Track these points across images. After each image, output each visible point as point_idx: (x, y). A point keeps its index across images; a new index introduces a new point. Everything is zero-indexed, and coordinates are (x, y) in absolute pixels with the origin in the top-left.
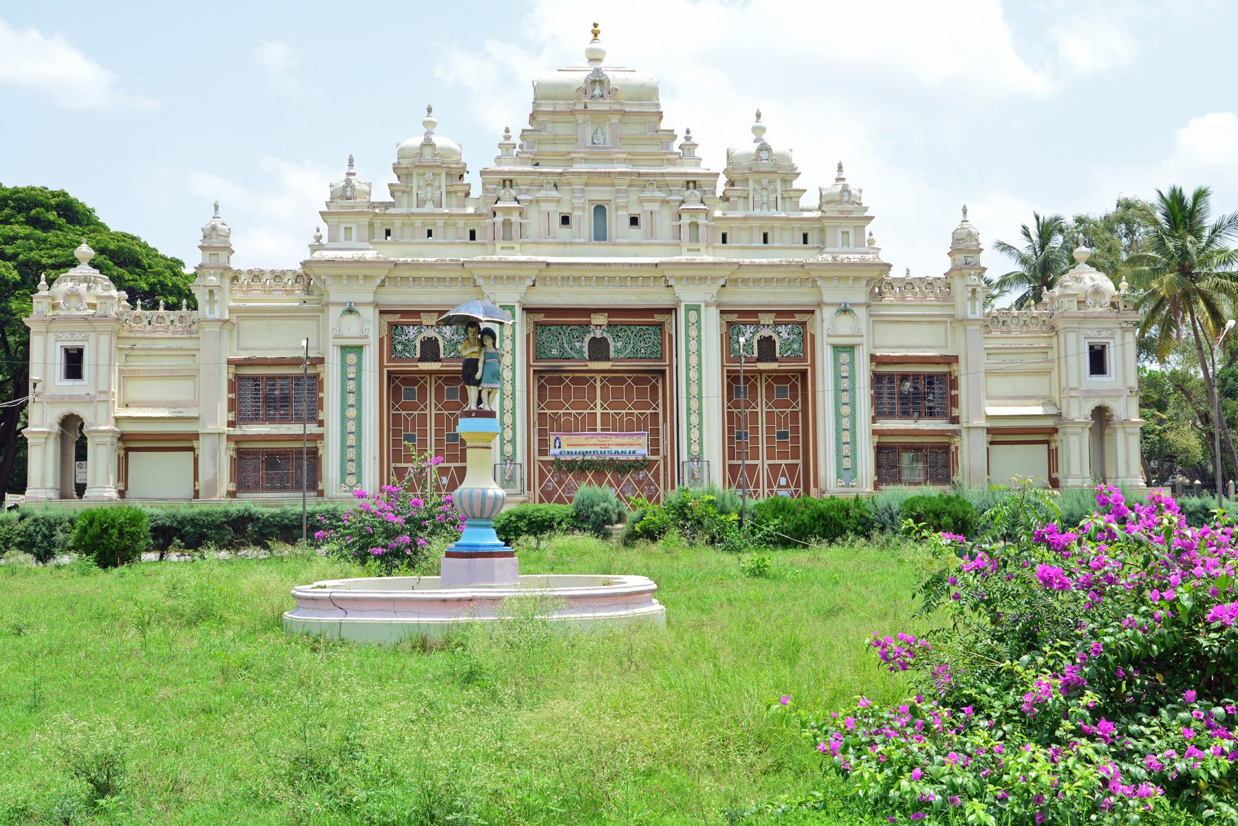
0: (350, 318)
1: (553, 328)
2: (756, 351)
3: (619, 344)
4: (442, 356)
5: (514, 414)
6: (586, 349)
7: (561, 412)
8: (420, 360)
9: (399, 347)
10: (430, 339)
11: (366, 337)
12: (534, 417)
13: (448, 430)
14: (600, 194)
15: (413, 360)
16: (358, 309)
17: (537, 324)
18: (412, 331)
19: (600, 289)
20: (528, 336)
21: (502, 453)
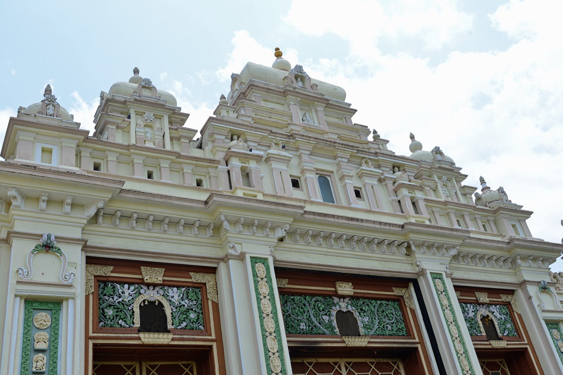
0: (46, 260)
1: (297, 298)
2: (482, 329)
3: (366, 319)
4: (170, 327)
6: (335, 323)
8: (139, 331)
9: (110, 312)
10: (152, 303)
11: (70, 286)
14: (326, 165)
15: (130, 329)
16: (56, 244)
18: (127, 292)
19: (347, 251)
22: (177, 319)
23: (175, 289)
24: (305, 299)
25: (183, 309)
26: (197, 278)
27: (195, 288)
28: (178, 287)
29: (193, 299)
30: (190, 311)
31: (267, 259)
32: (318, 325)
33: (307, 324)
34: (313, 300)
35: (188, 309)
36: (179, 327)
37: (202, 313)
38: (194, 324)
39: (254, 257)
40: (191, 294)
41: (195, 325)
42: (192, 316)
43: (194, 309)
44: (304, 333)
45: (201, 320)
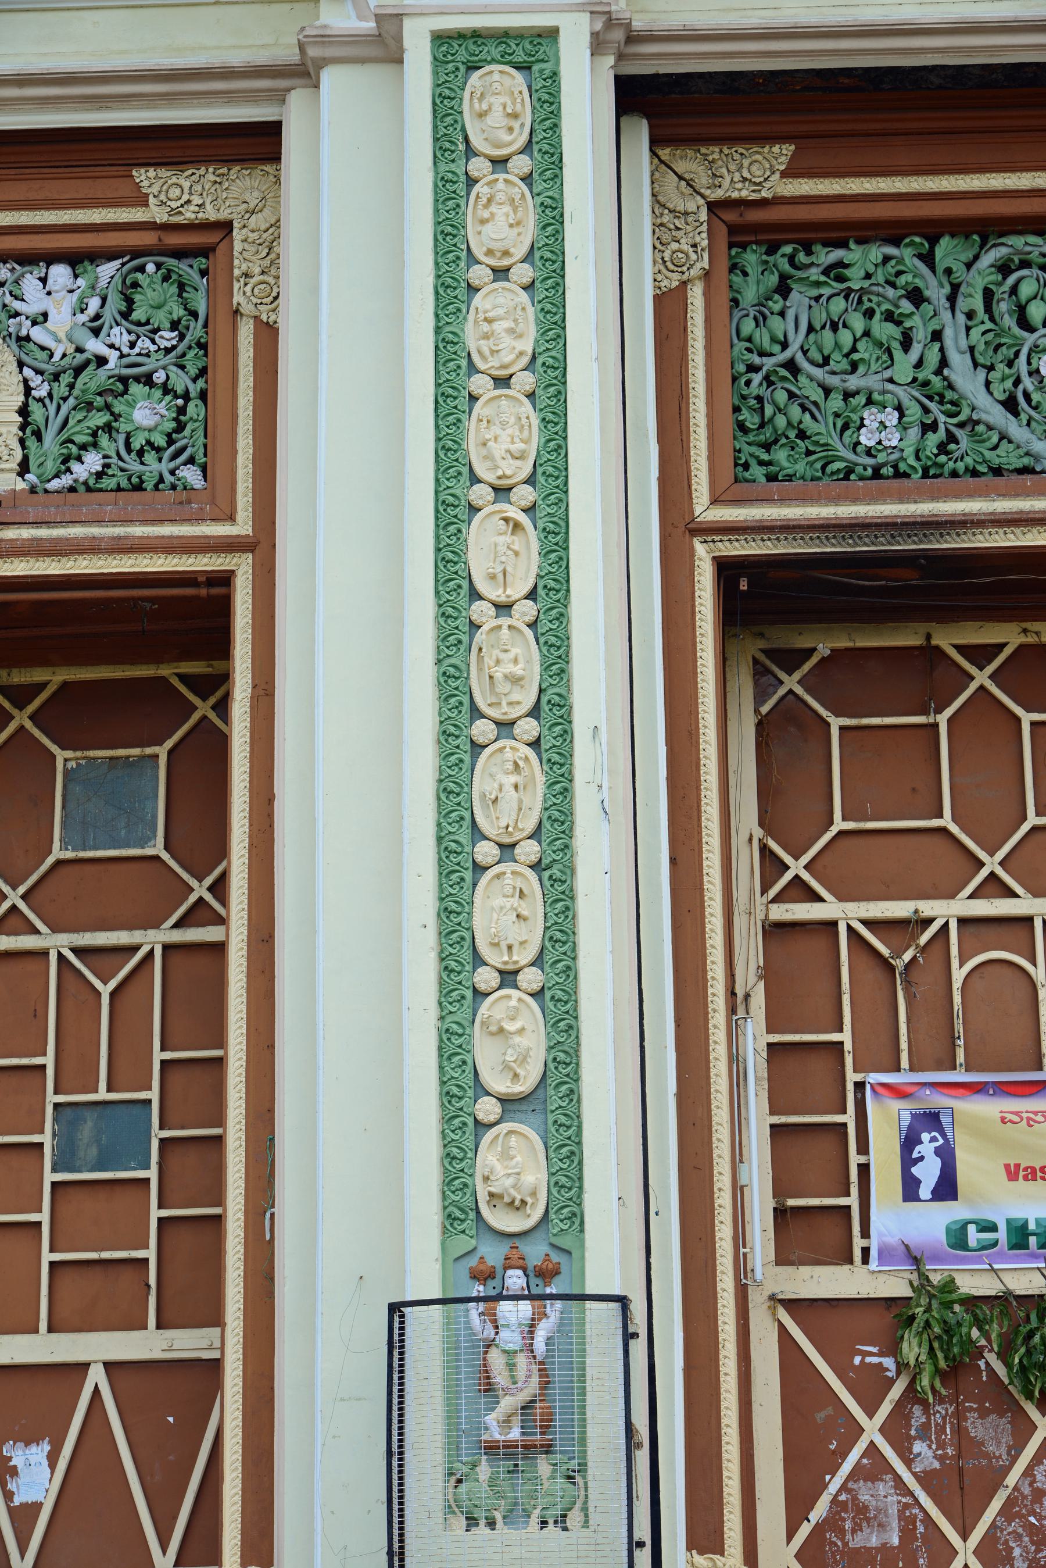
1: (864, 258)
5: (556, 874)
7: (943, 910)
12: (737, 956)
13: (74, 1071)
17: (741, 228)
20: (669, 308)
21: (460, 1212)
22: (49, 437)
23: (60, 273)
24: (928, 259)
25: (93, 380)
26: (171, 195)
27: (179, 254)
28: (75, 260)
29: (161, 318)
30: (136, 389)
31: (553, 33)
32: (997, 415)
33: (914, 412)
34: (989, 258)
35: (124, 380)
36: (55, 484)
37: (203, 395)
38: (150, 457)
39: (461, 36)
40: (155, 296)
41: (154, 466)
42: (146, 413)
43: (159, 377)
44: (877, 474)
45: (192, 438)
